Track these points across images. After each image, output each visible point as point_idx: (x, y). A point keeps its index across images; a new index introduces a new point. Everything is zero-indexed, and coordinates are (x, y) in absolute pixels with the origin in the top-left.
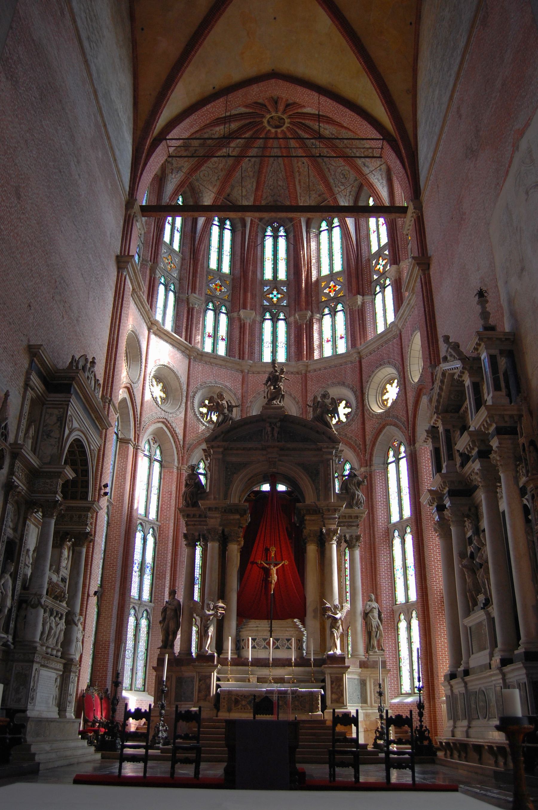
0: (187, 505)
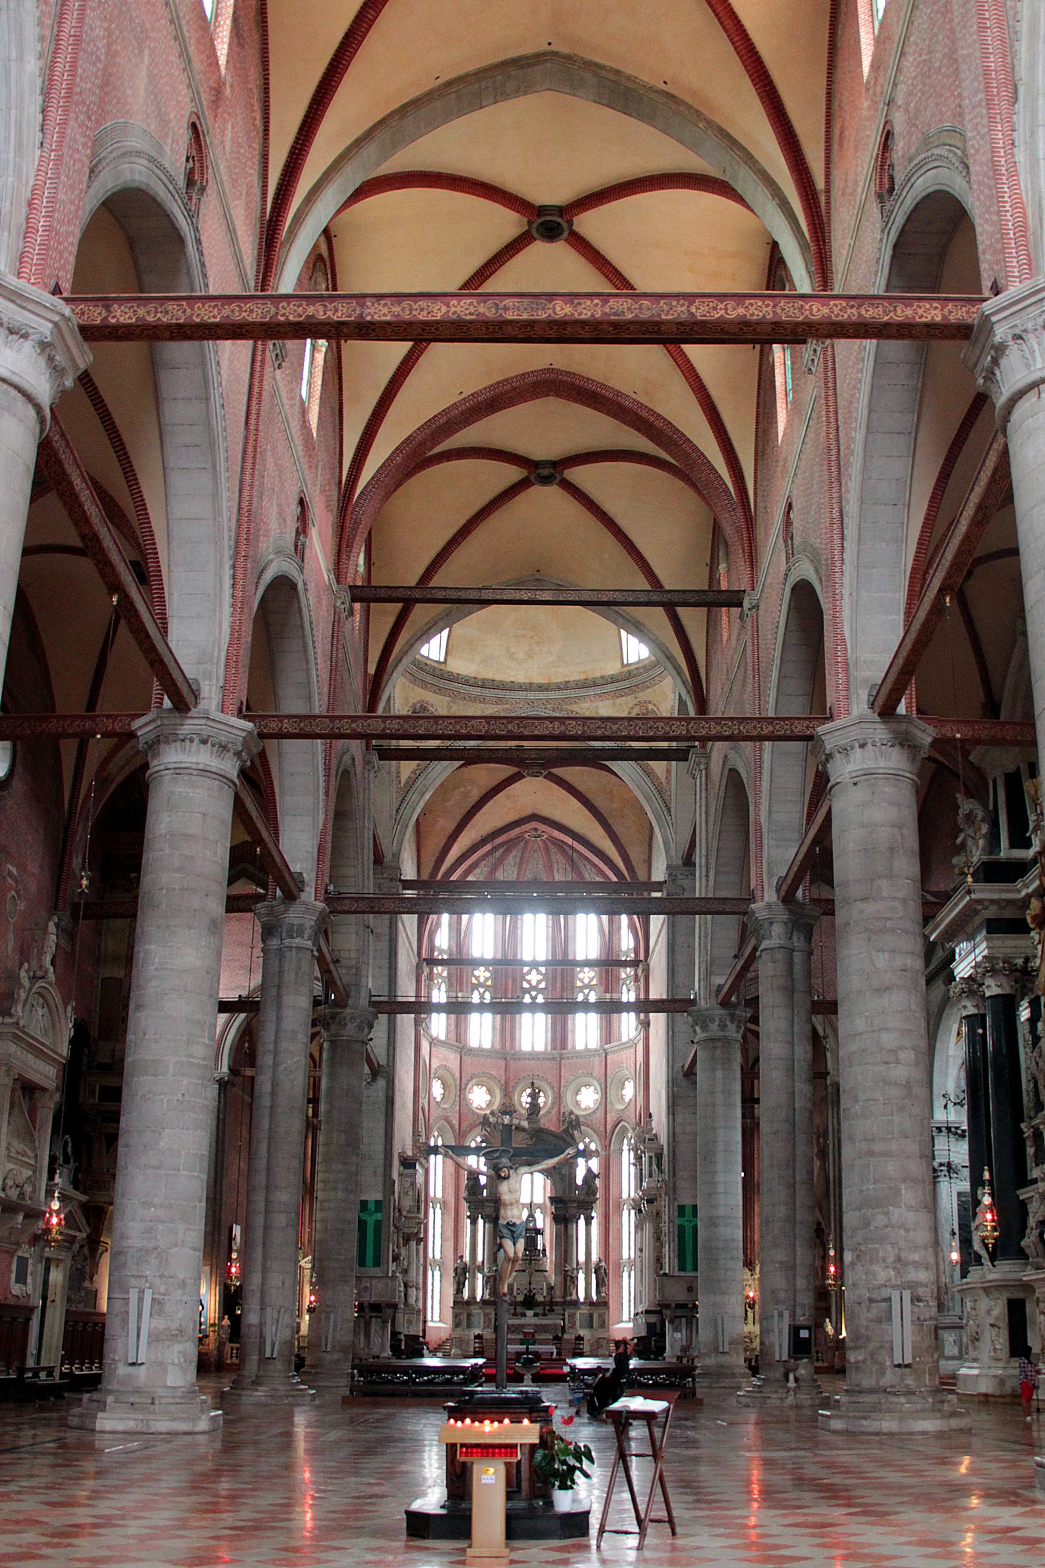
0: (469, 1194)
